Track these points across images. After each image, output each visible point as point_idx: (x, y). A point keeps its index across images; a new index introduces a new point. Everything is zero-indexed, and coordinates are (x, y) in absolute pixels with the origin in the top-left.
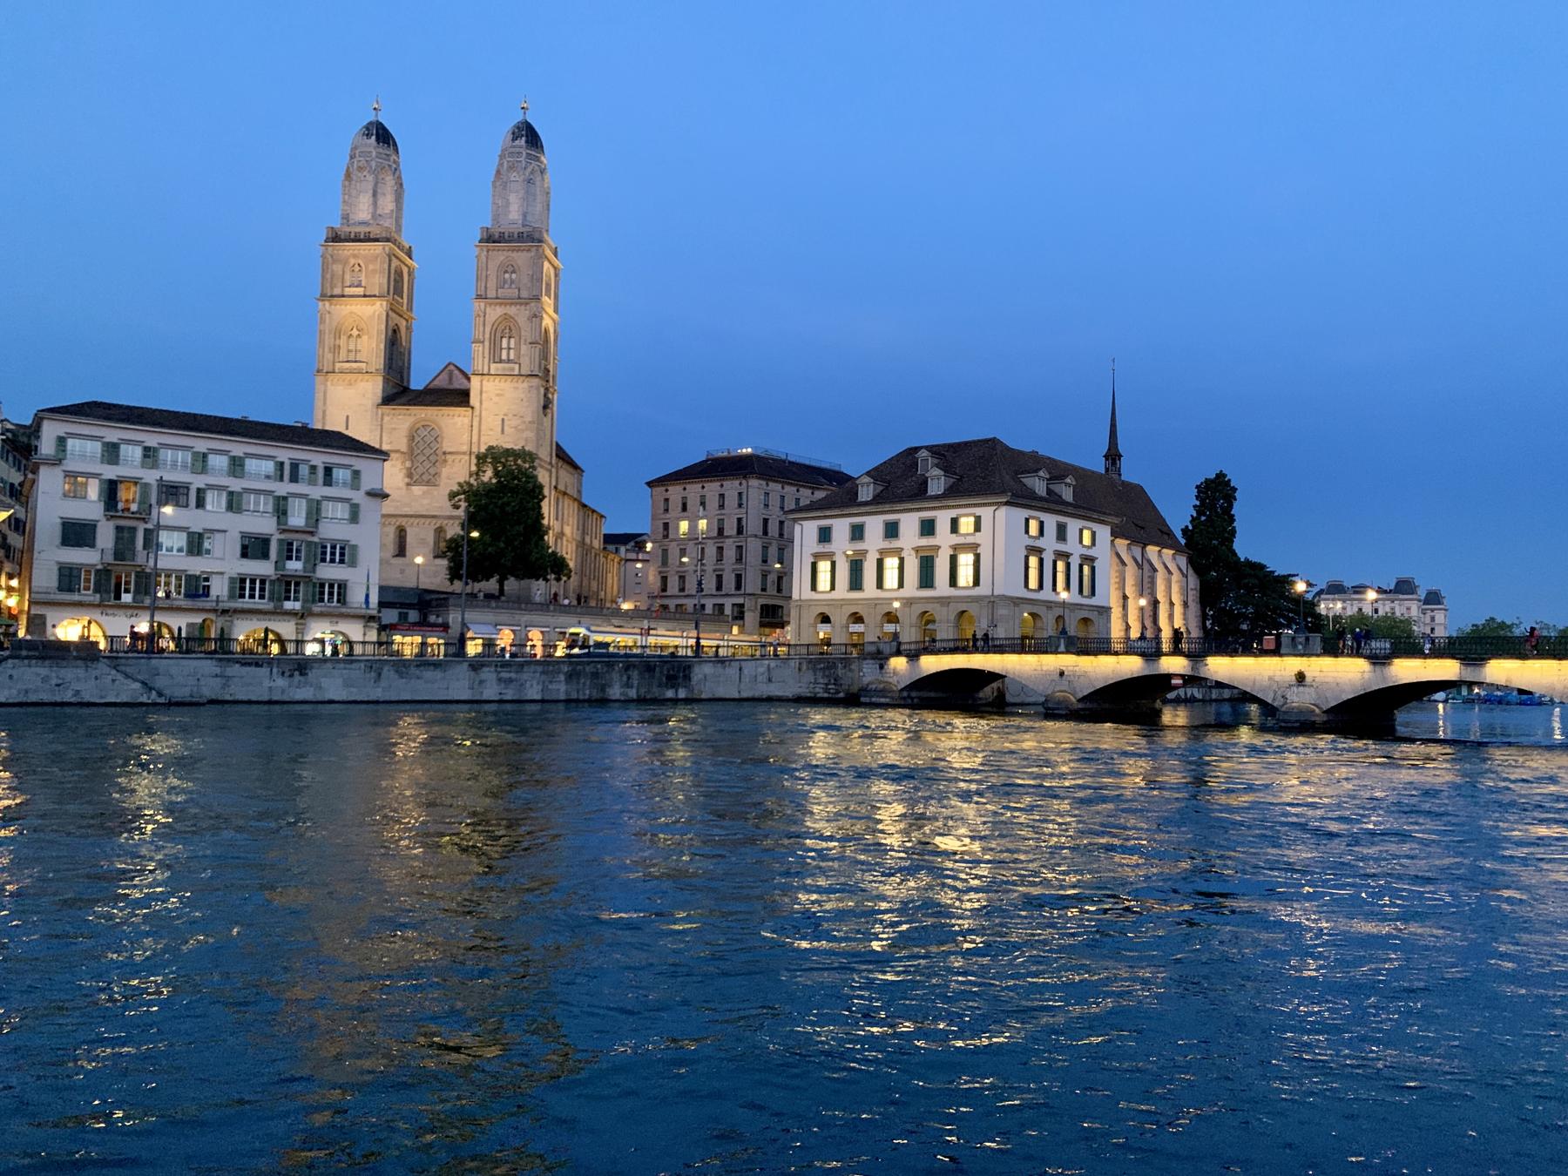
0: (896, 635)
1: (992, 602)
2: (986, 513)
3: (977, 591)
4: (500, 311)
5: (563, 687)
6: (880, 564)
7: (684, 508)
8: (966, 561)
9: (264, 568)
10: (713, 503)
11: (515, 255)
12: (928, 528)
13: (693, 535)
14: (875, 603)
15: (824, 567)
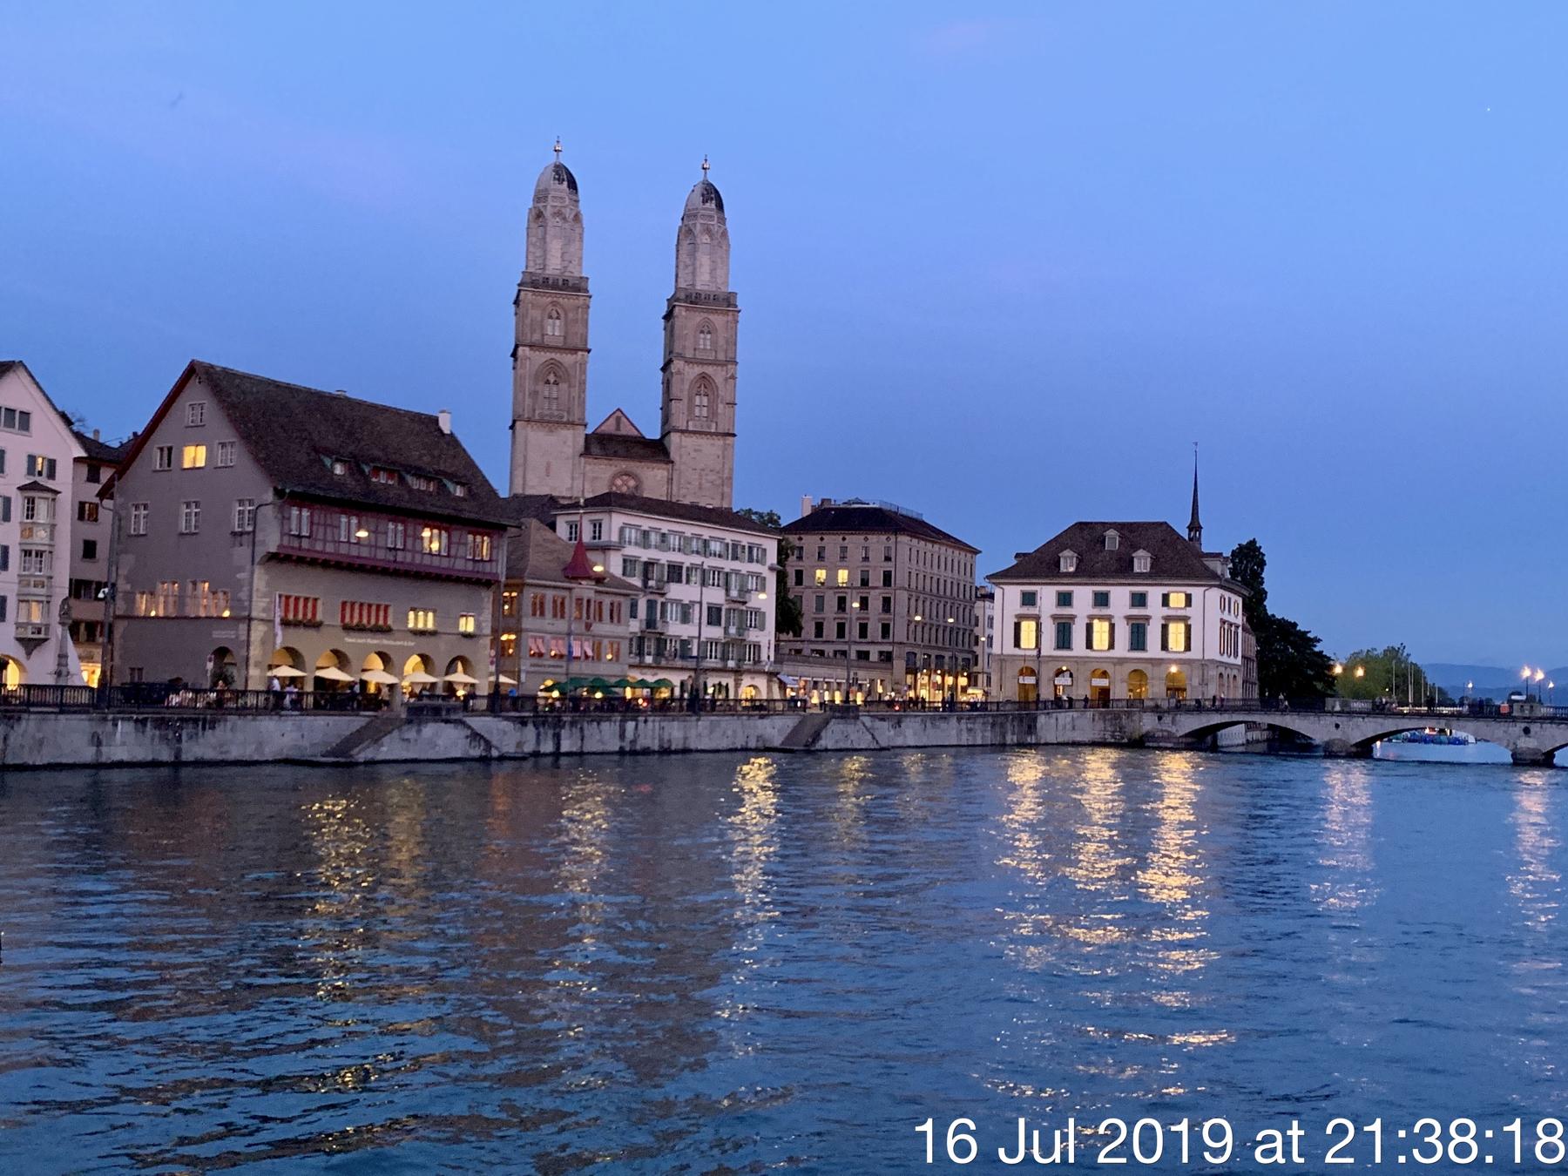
0: (1105, 692)
1: (1204, 664)
2: (1197, 592)
3: (1188, 655)
4: (698, 370)
5: (988, 734)
6: (1089, 628)
7: (821, 557)
8: (1176, 632)
9: (716, 632)
10: (856, 554)
11: (711, 317)
12: (1139, 600)
13: (831, 584)
14: (1080, 661)
15: (1028, 628)
